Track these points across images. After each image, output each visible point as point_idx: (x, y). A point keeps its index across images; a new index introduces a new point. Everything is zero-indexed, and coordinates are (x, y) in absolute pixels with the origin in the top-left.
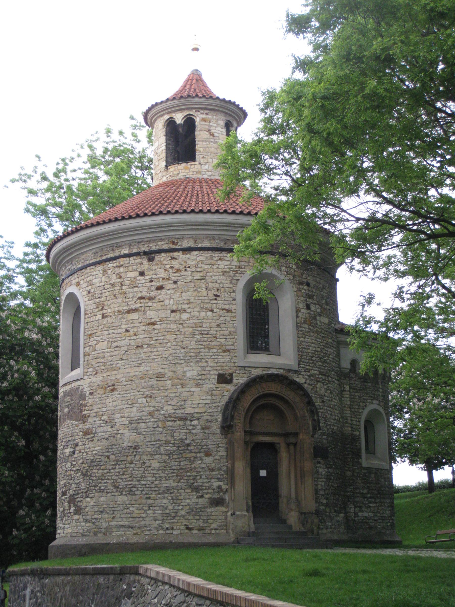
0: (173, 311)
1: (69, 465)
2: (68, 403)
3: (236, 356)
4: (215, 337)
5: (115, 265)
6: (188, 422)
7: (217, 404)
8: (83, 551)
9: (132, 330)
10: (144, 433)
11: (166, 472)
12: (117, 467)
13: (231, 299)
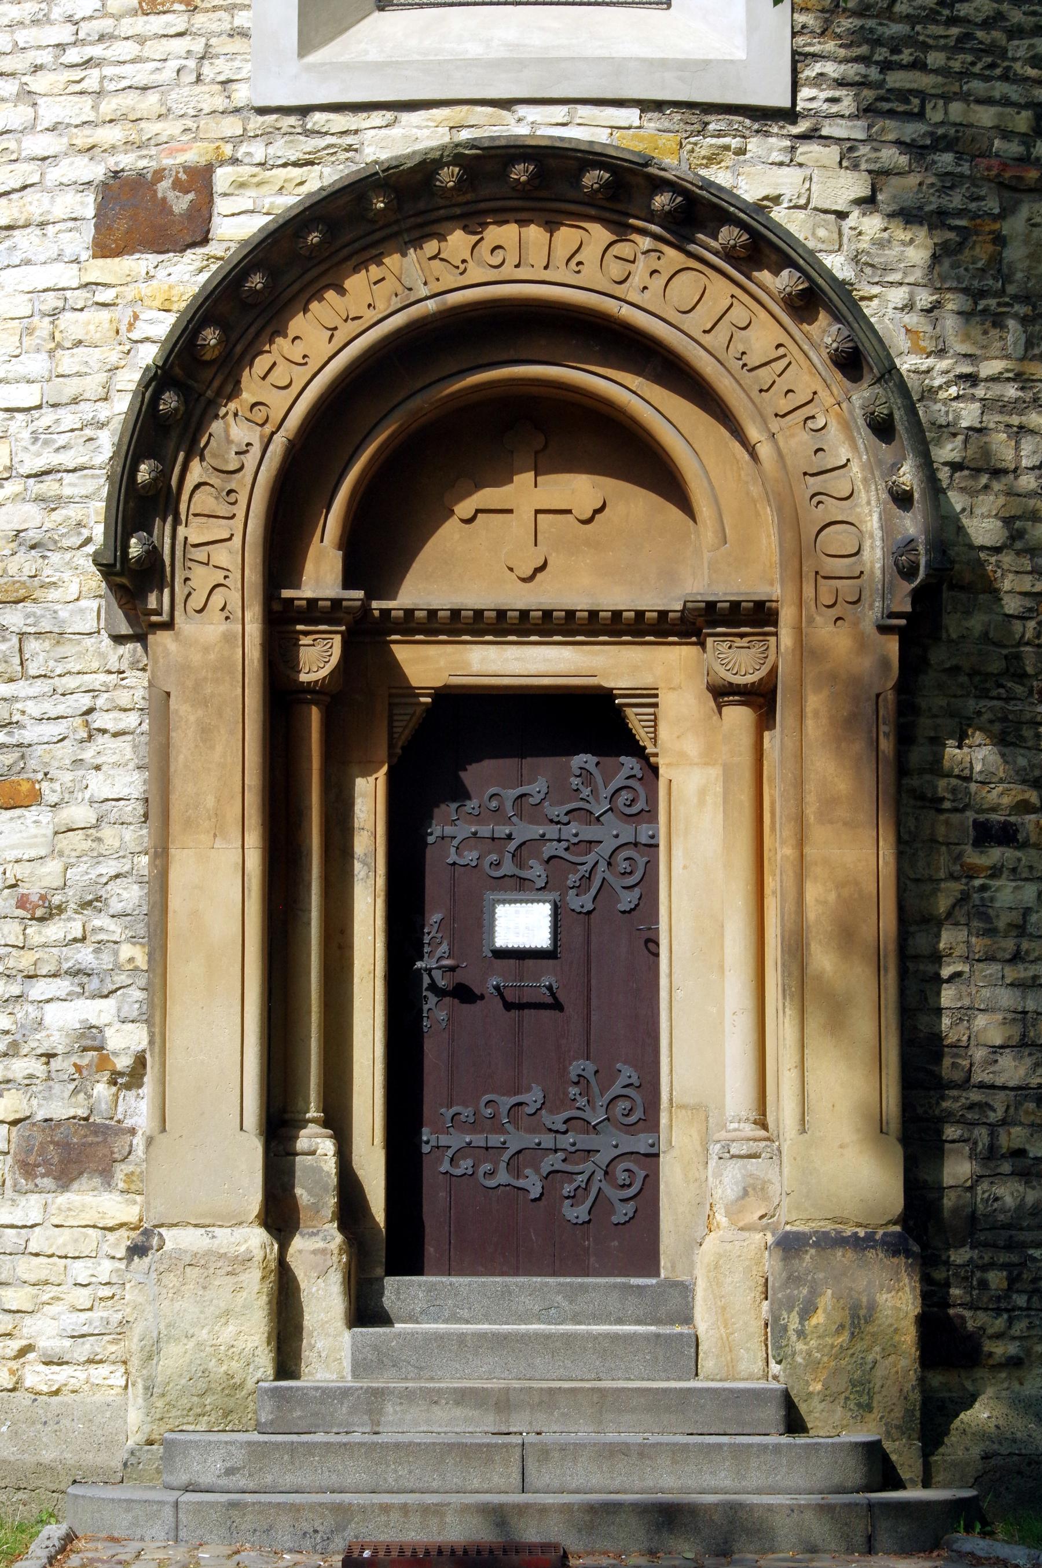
3: (243, 34)
7: (86, 410)
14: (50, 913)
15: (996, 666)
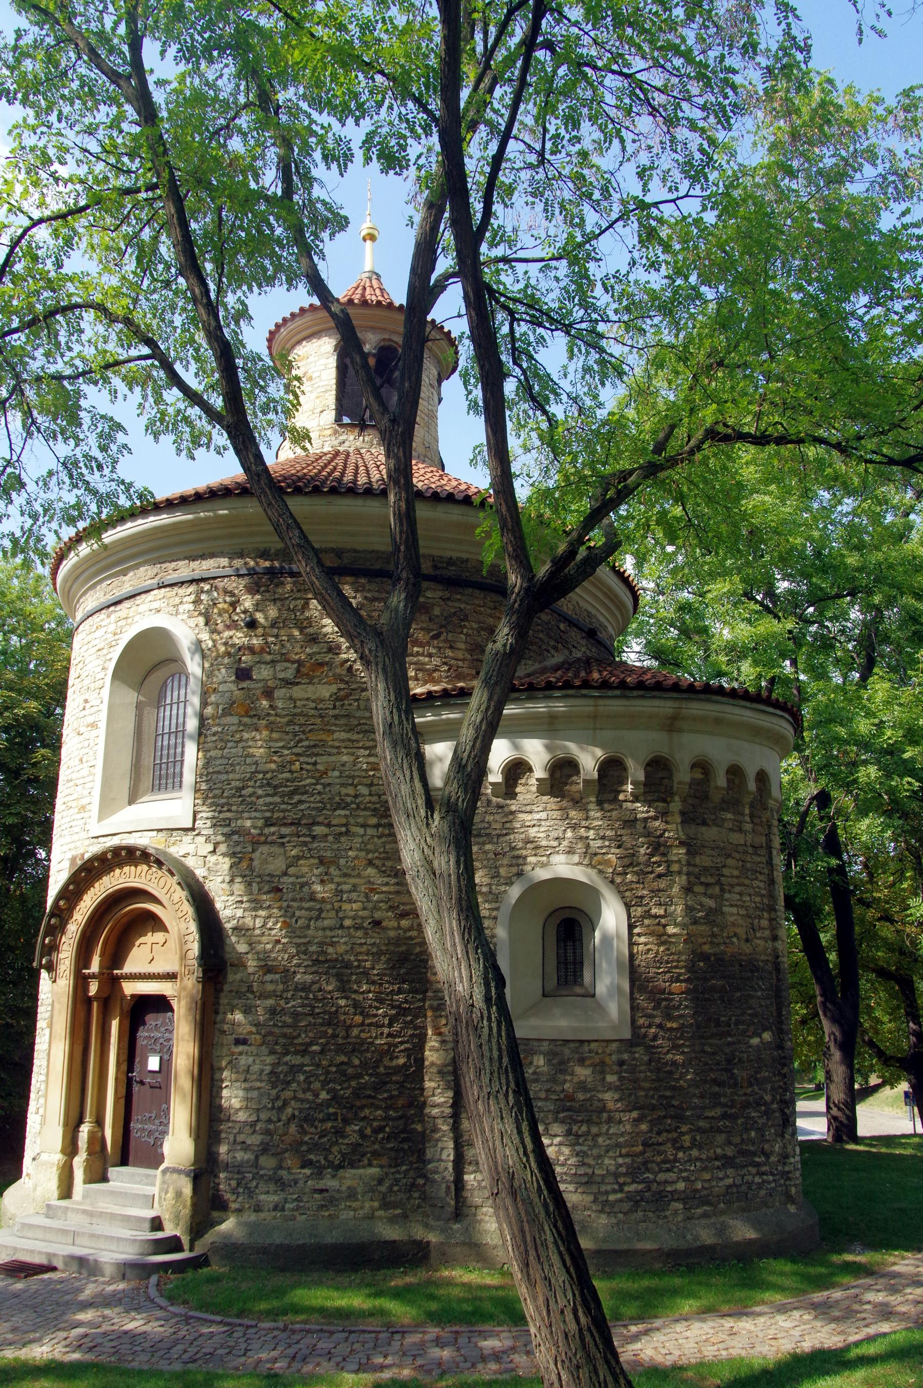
15: (244, 989)
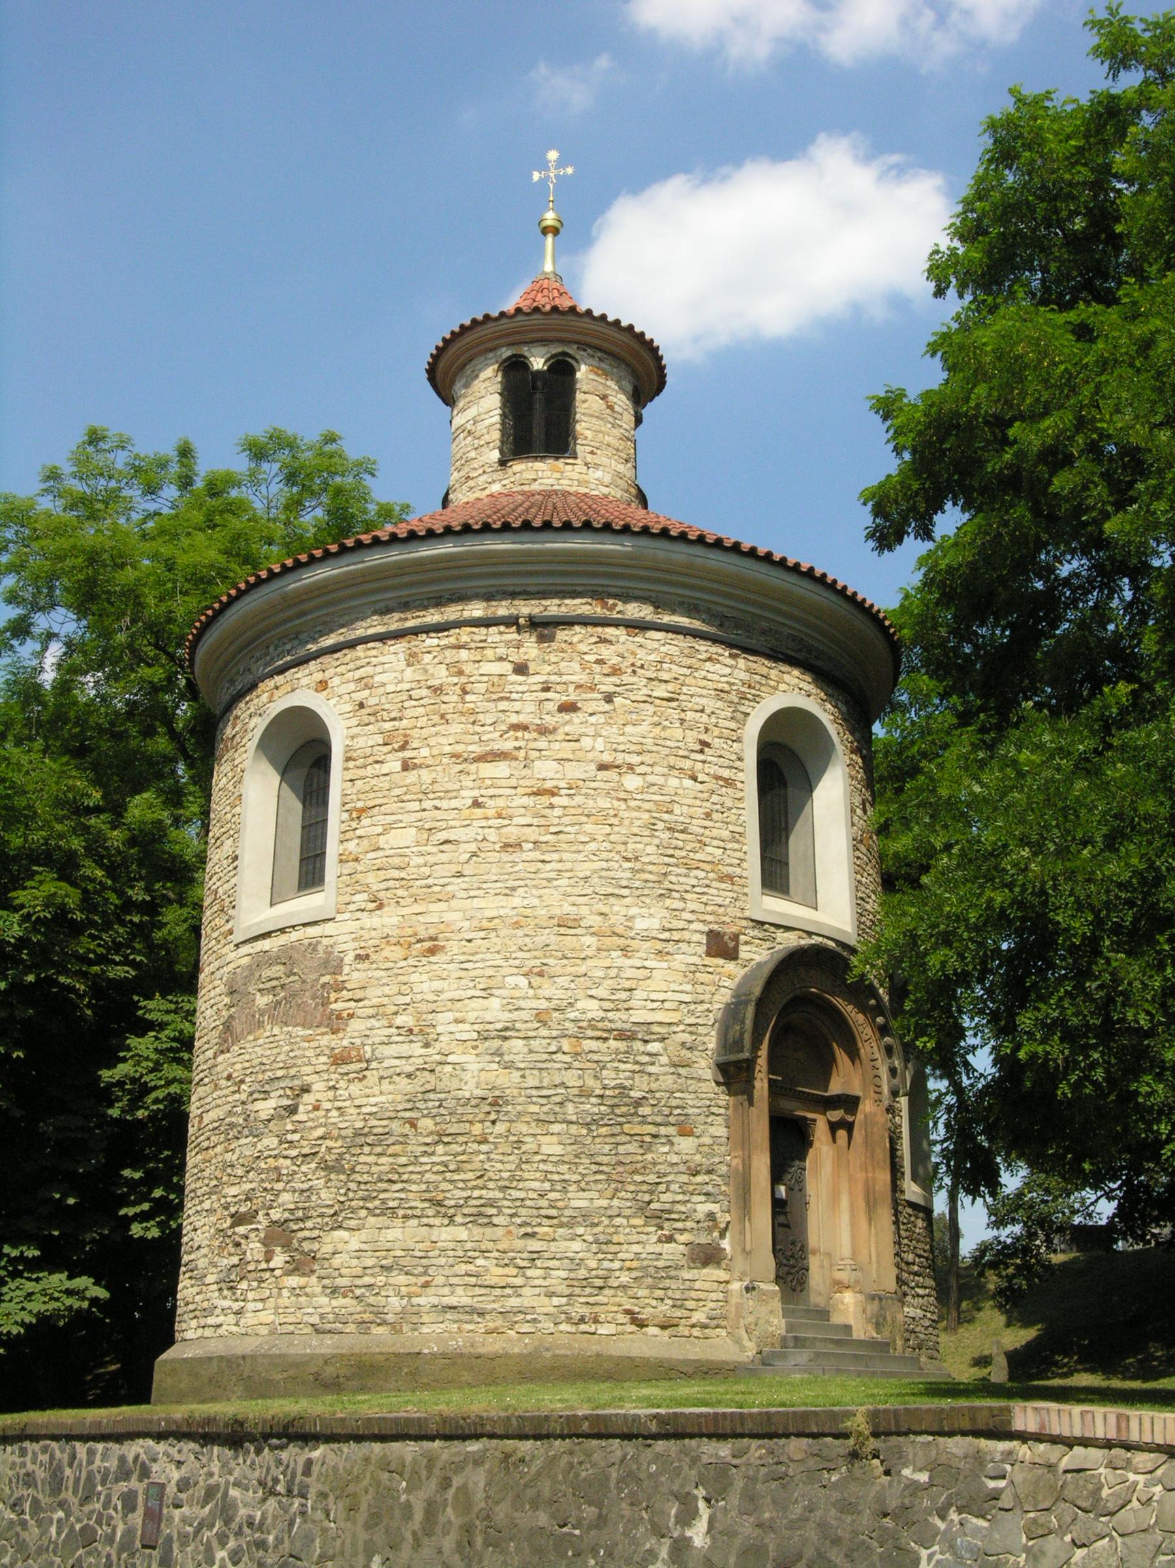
0: (603, 767)
1: (271, 1142)
2: (274, 983)
4: (700, 842)
5: (442, 643)
6: (638, 1045)
7: (706, 1006)
8: (329, 1371)
9: (490, 803)
10: (522, 1065)
11: (581, 1169)
12: (440, 1149)
13: (734, 757)
14: (697, 1173)
